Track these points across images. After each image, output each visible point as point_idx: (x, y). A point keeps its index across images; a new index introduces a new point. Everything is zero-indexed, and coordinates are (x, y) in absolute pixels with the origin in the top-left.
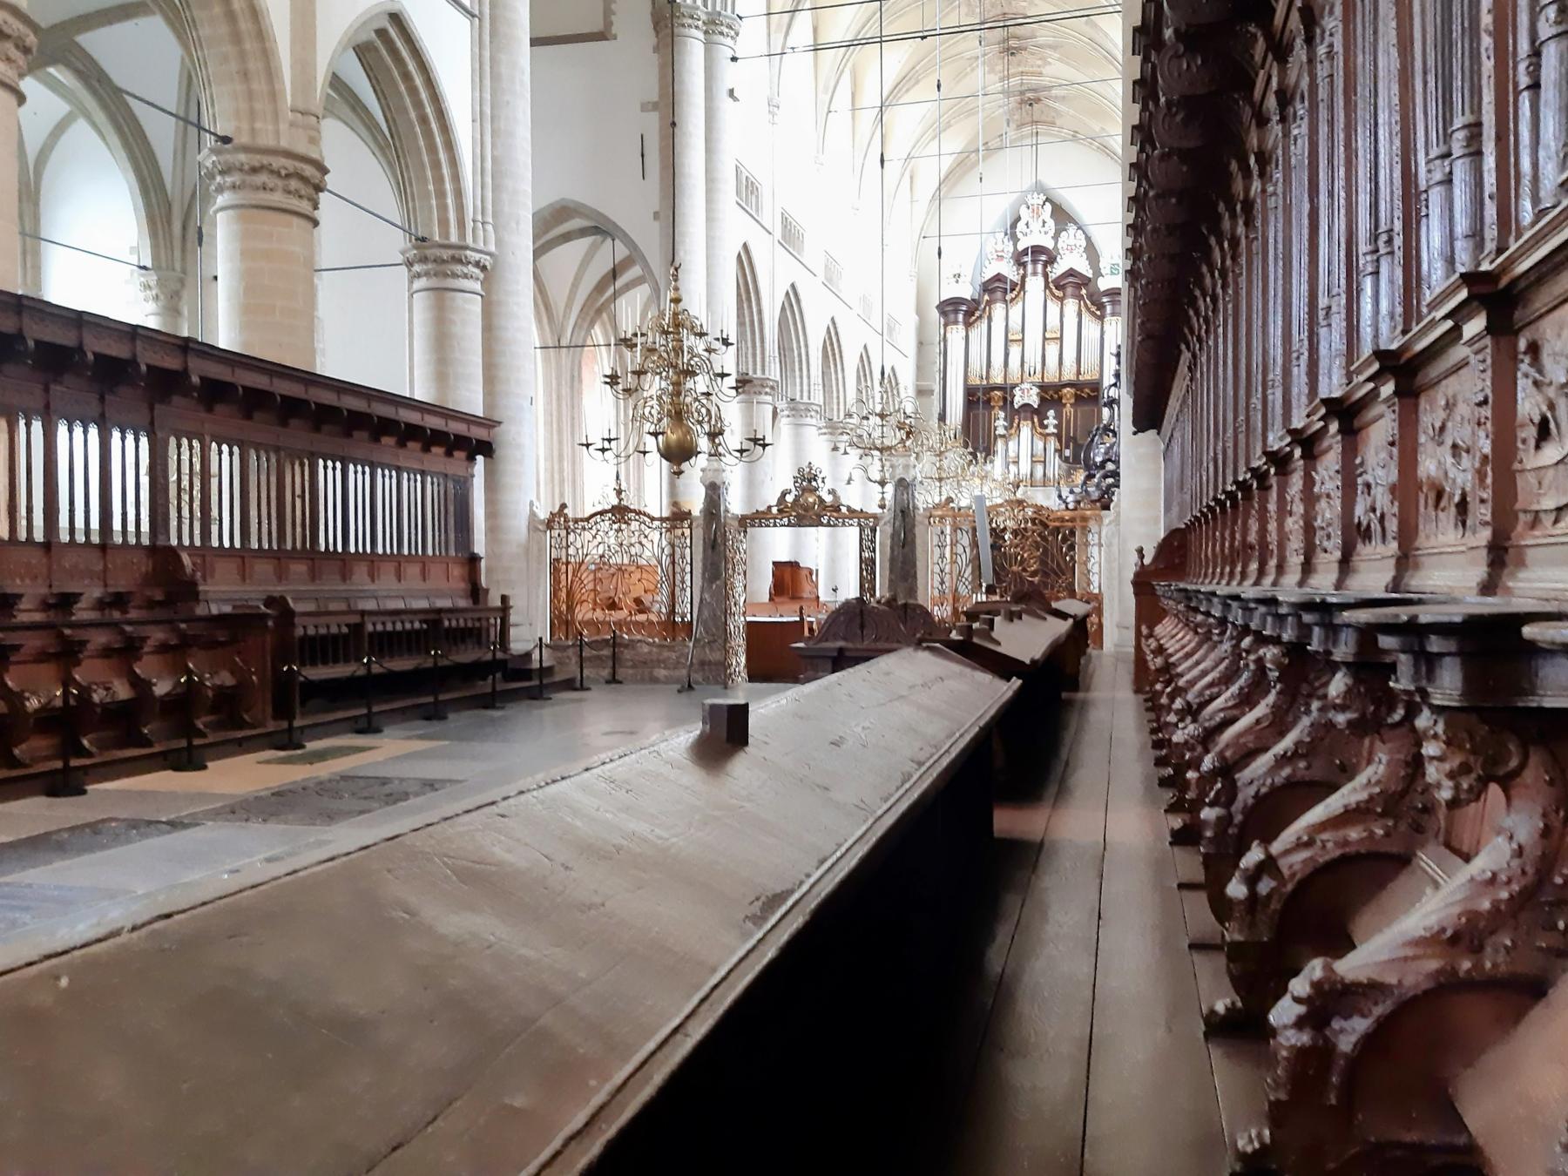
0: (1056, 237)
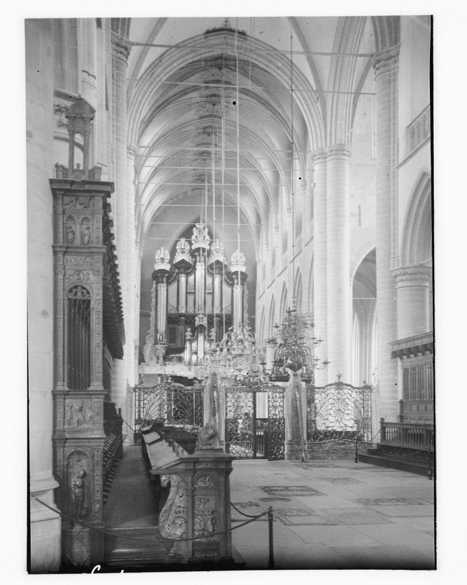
0: (210, 244)
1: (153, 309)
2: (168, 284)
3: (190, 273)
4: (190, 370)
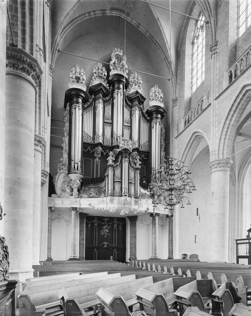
1: (66, 134)
2: (84, 109)
3: (107, 101)
4: (112, 201)
